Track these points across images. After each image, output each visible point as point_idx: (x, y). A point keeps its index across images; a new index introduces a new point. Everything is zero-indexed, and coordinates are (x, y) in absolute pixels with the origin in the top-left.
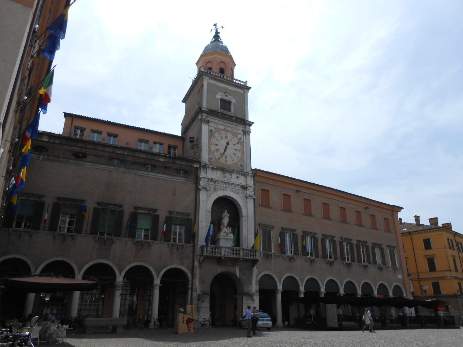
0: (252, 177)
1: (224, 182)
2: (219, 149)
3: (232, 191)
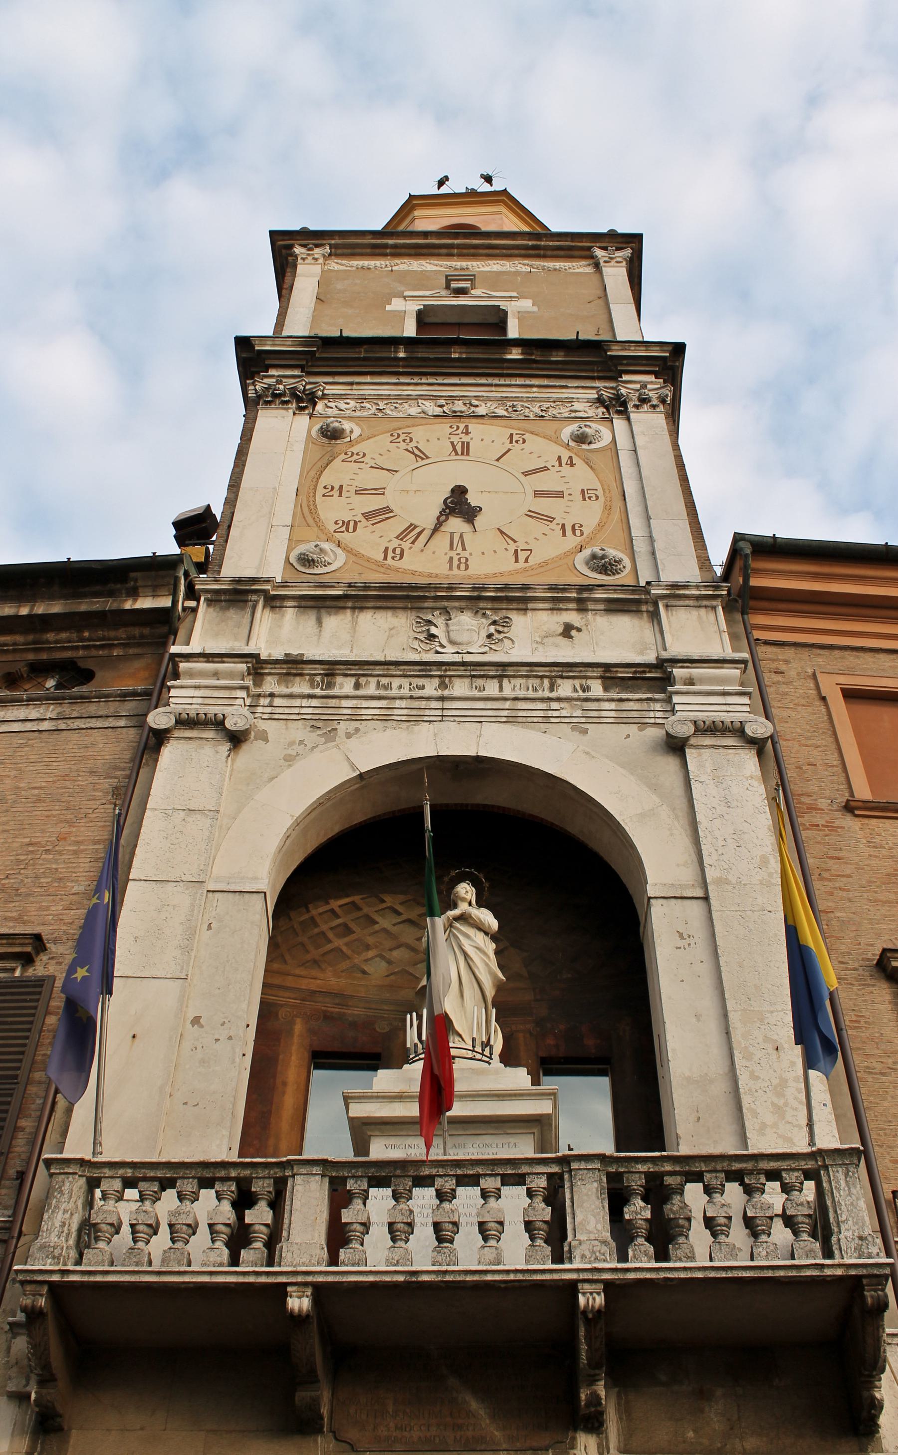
0: (714, 608)
1: (424, 668)
2: (392, 507)
3: (512, 720)
